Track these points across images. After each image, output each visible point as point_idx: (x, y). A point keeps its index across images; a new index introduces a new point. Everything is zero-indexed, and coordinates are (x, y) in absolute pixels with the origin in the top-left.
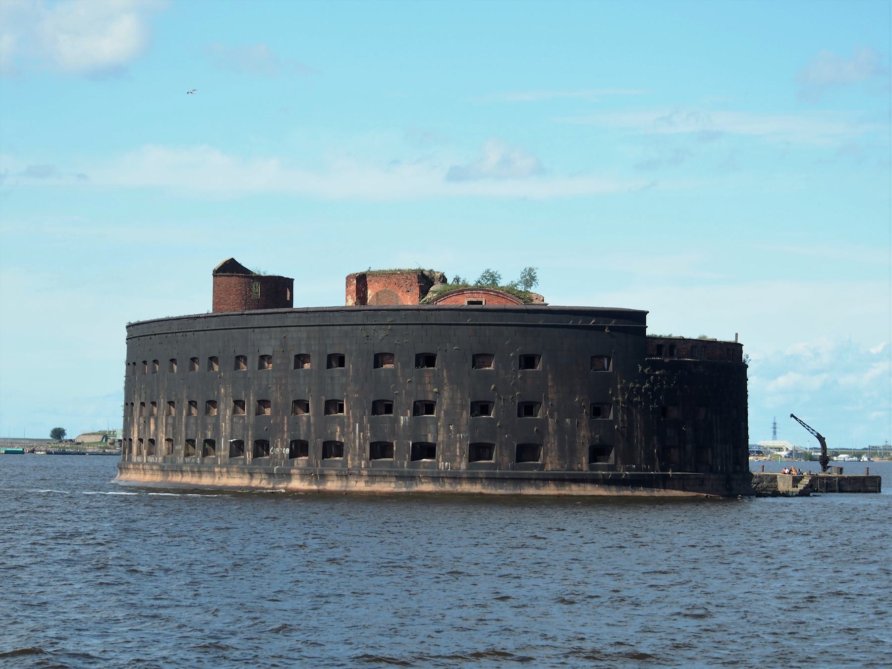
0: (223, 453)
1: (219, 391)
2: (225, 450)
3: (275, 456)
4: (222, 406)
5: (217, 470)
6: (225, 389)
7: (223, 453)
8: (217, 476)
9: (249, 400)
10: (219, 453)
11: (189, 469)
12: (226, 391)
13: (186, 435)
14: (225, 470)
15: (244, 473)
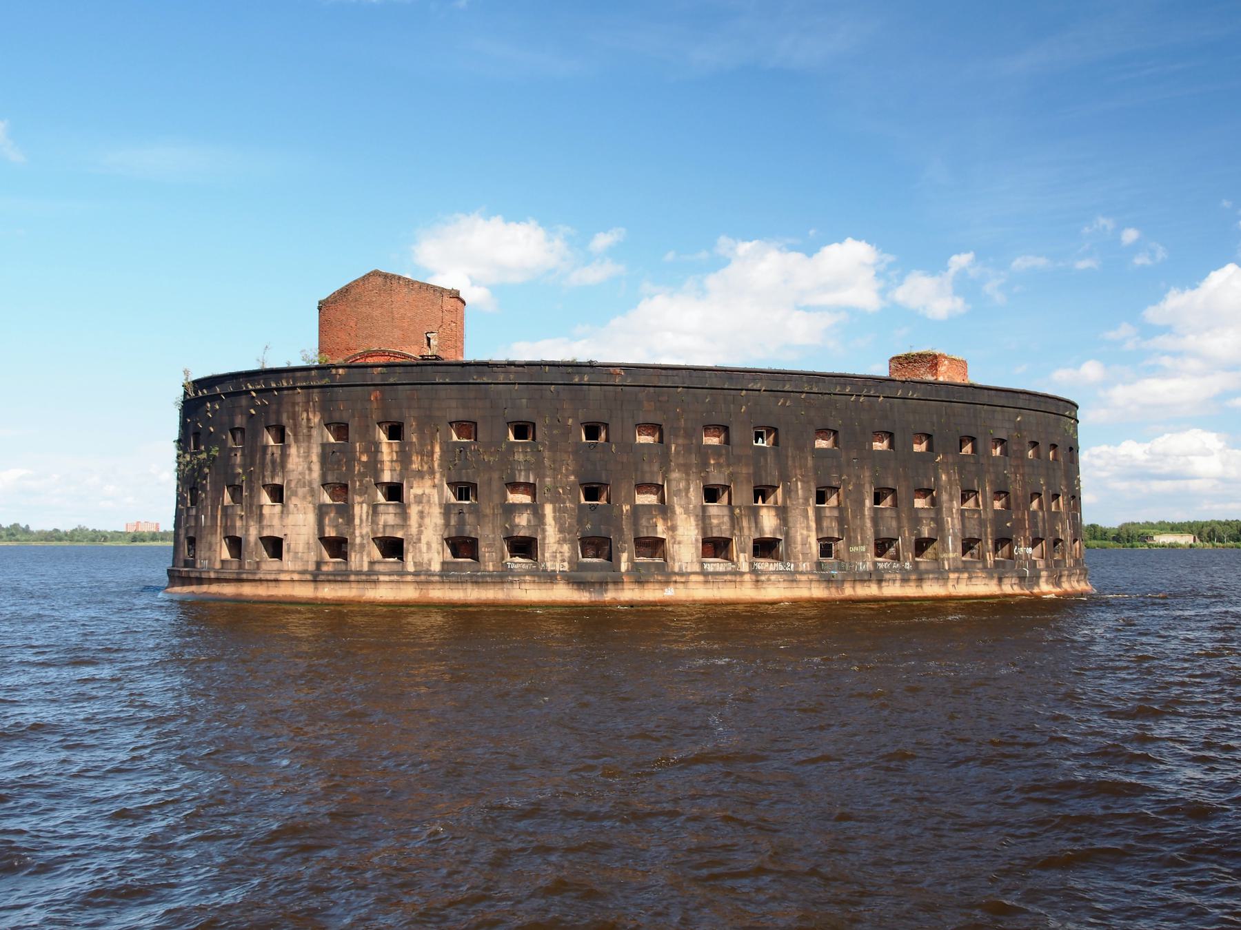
0: (951, 555)
1: (937, 478)
2: (955, 551)
3: (1019, 557)
4: (945, 497)
5: (952, 576)
6: (948, 474)
7: (951, 555)
8: (950, 584)
9: (984, 491)
10: (945, 555)
11: (898, 576)
12: (949, 480)
13: (877, 532)
14: (966, 575)
15: (992, 578)
